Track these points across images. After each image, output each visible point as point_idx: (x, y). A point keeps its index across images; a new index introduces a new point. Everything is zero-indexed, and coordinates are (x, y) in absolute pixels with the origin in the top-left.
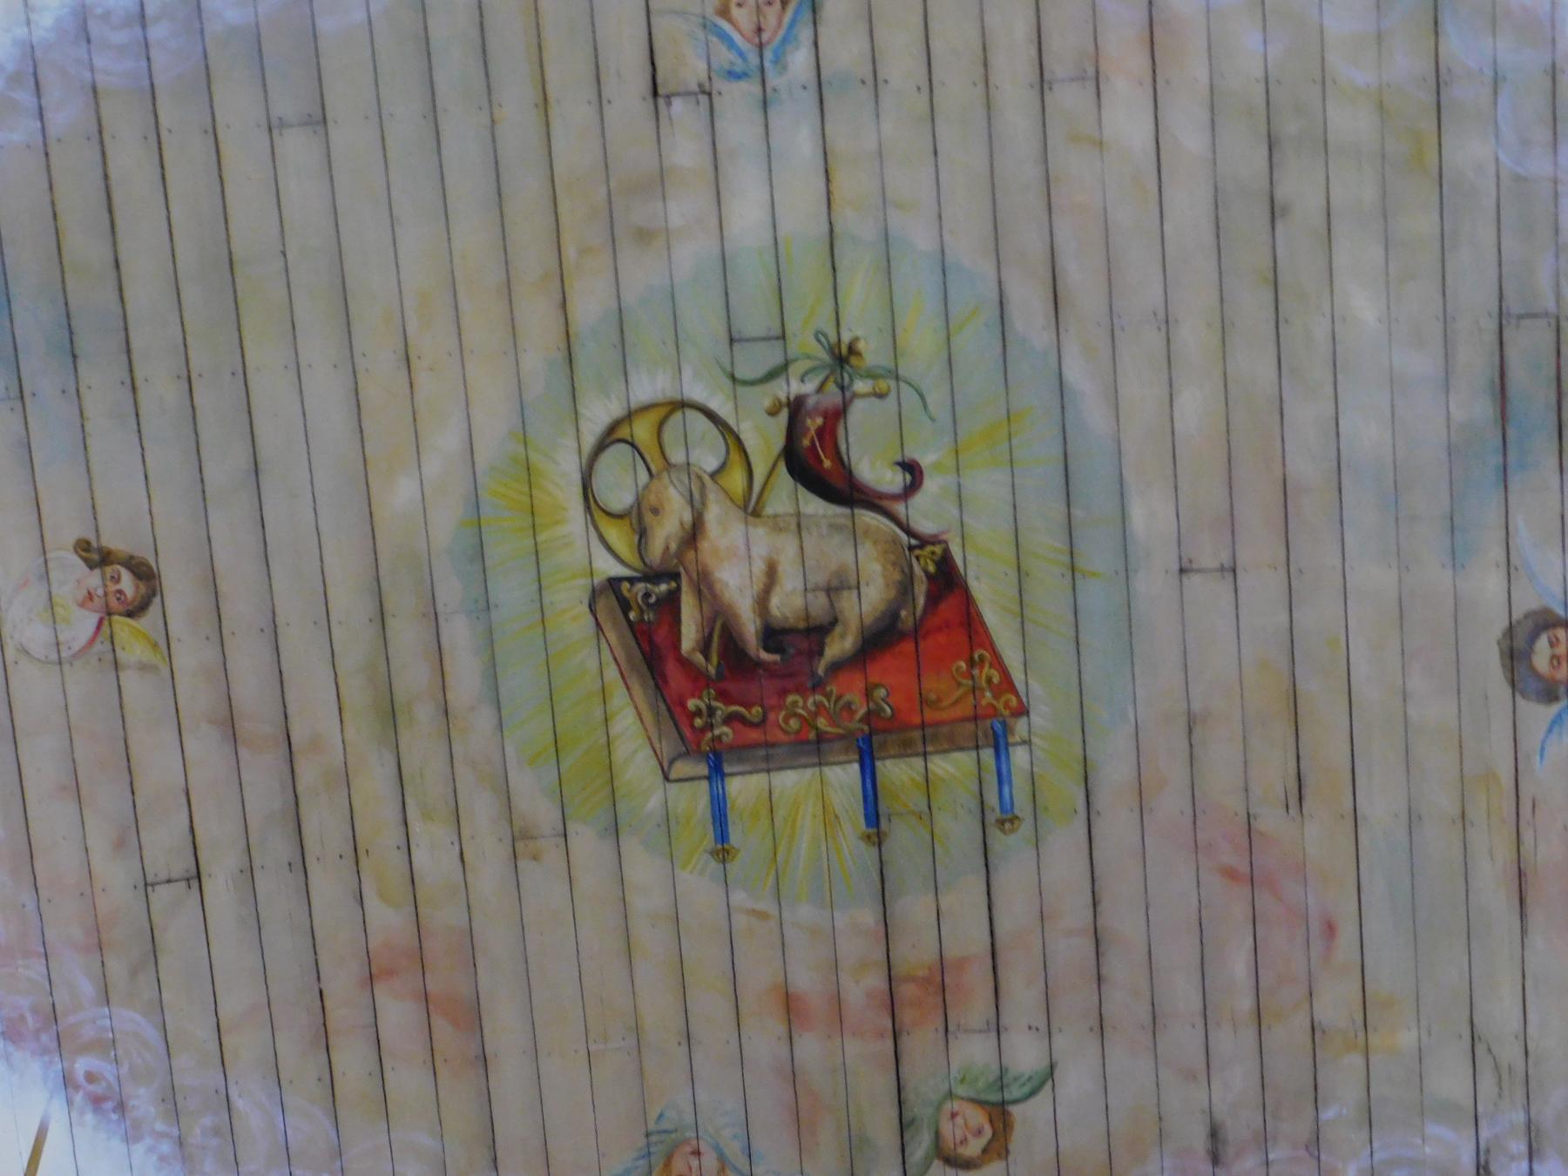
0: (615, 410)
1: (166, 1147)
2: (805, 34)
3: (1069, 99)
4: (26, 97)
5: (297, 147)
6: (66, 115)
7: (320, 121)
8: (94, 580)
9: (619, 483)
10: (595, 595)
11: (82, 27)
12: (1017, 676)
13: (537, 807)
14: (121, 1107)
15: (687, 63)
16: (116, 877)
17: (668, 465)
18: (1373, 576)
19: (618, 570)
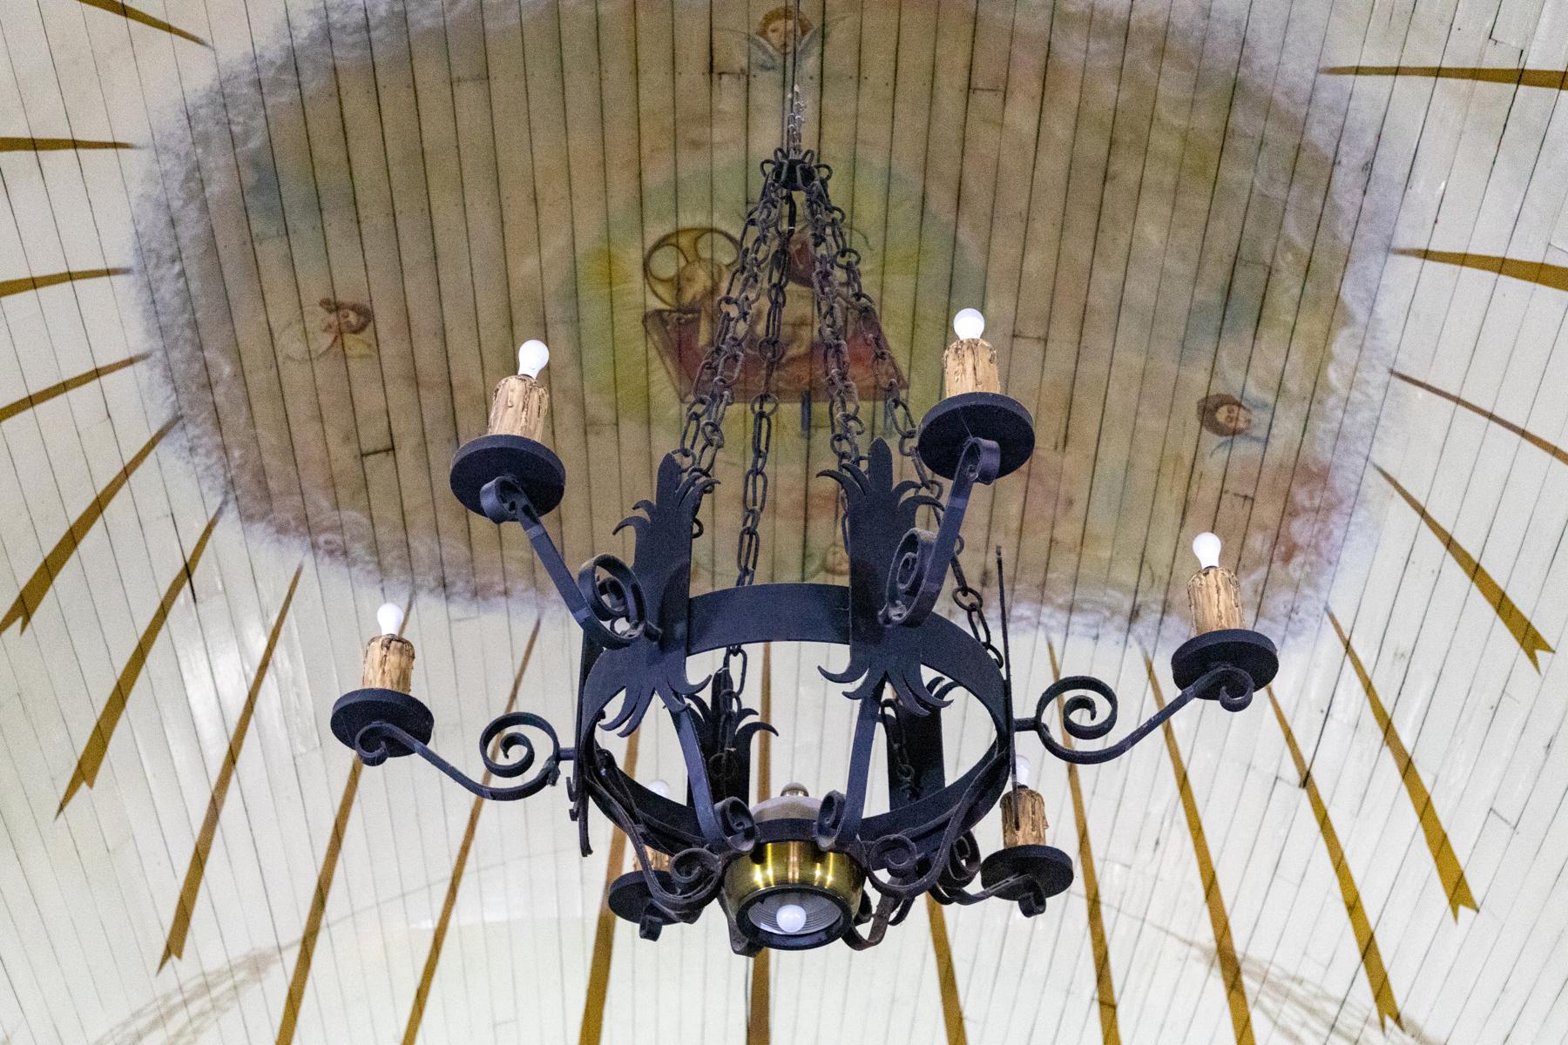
0: (668, 228)
1: (371, 567)
2: (816, 50)
3: (986, 101)
4: (289, 77)
5: (469, 94)
6: (314, 83)
7: (485, 77)
8: (332, 318)
9: (666, 264)
10: (644, 321)
11: (327, 34)
12: (905, 372)
13: (599, 407)
14: (345, 553)
15: (734, 54)
16: (343, 456)
17: (699, 259)
18: (1130, 358)
19: (660, 305)
